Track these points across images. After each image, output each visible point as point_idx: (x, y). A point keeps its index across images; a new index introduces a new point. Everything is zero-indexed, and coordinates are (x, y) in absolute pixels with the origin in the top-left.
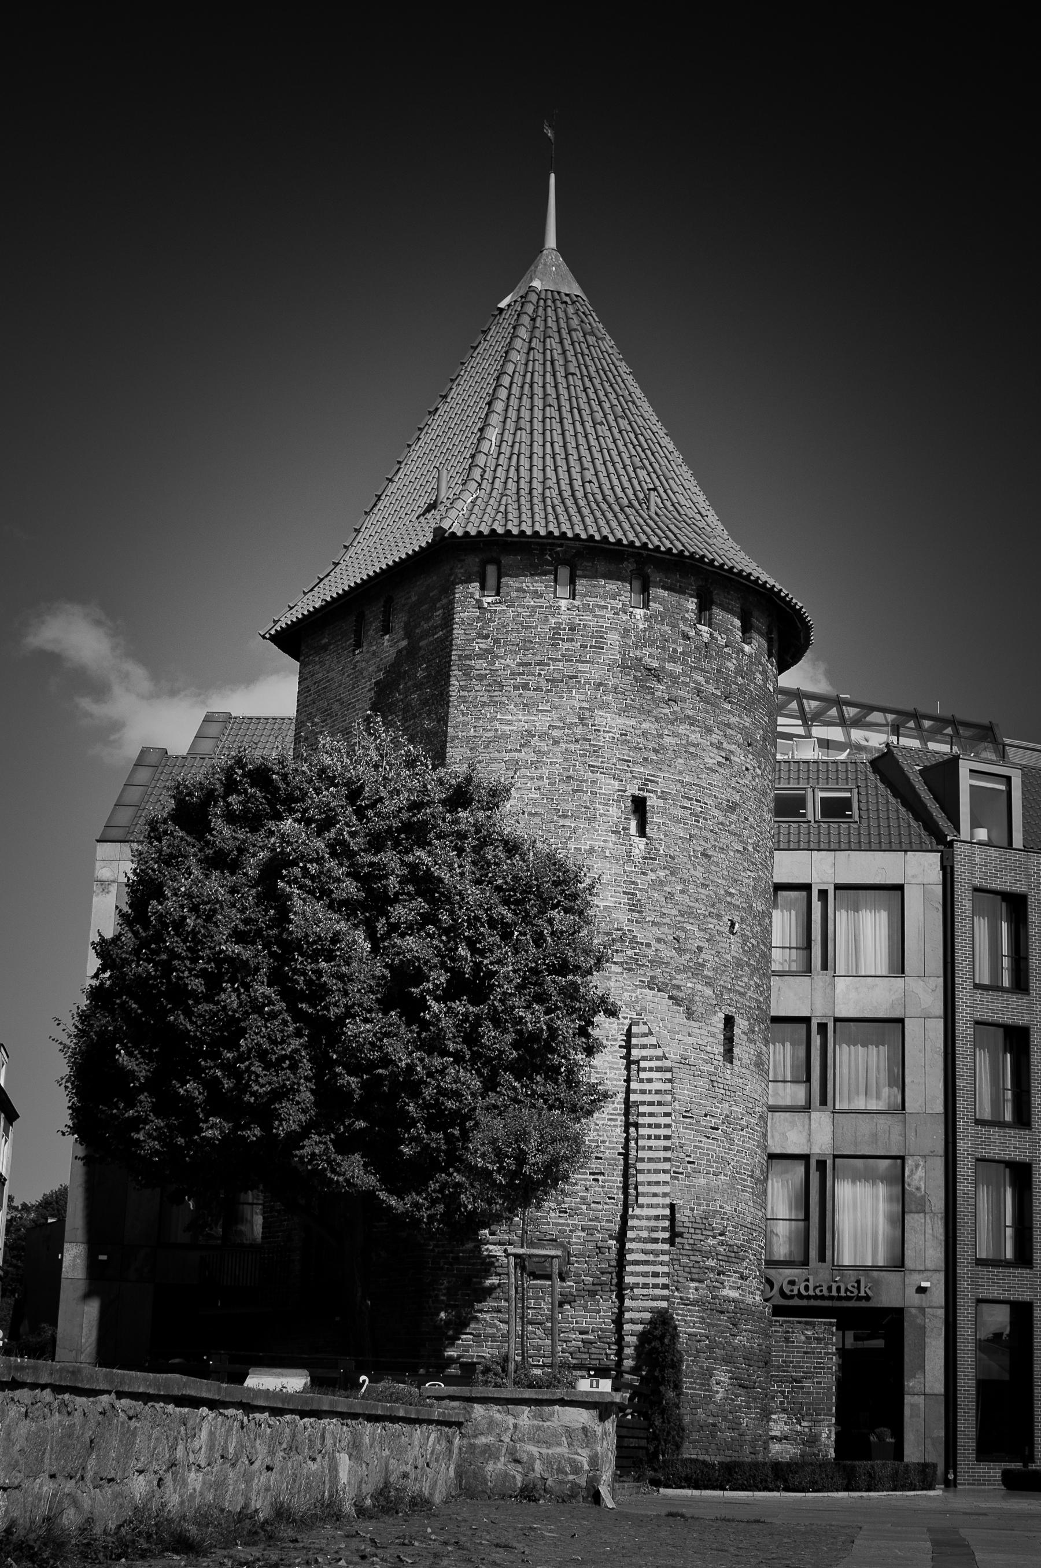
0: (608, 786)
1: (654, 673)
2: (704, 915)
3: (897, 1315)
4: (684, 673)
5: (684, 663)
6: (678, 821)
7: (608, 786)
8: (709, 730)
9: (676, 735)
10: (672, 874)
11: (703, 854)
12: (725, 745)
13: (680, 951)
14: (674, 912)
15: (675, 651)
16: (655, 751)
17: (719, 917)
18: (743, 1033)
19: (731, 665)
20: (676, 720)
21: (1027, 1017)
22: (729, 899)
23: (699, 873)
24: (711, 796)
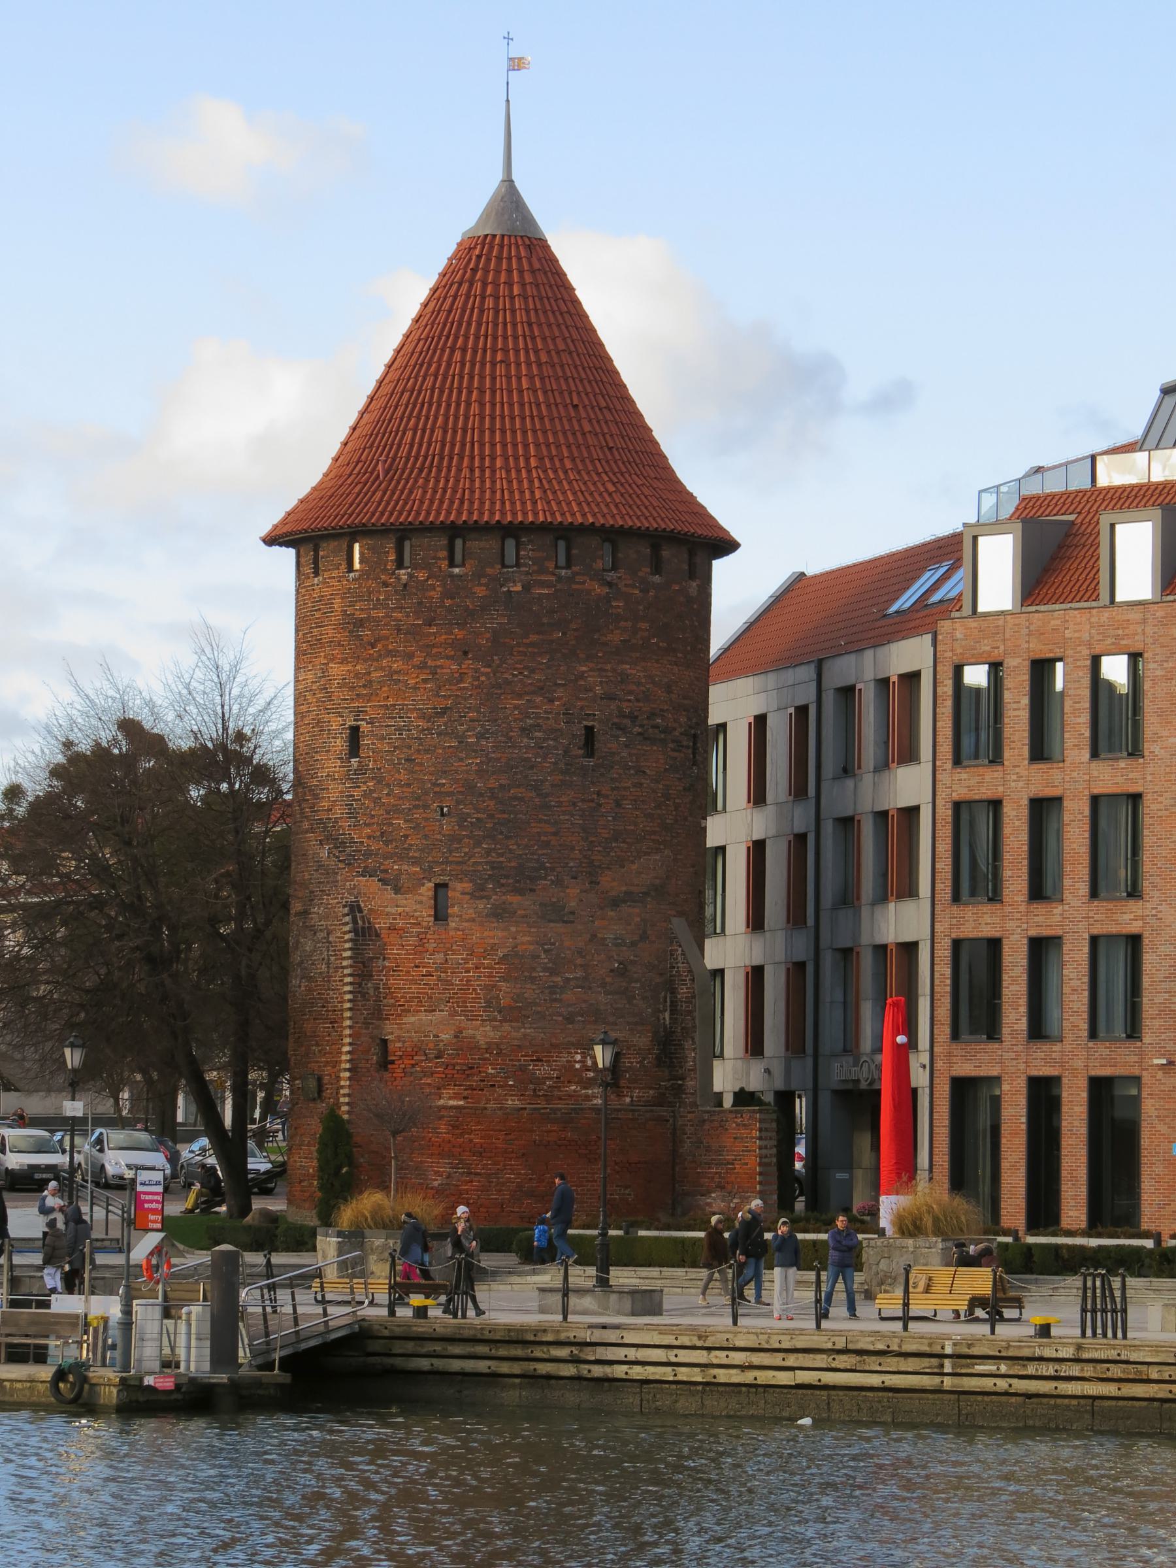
0: (336, 723)
2: (410, 810)
4: (387, 616)
5: (387, 607)
6: (383, 738)
7: (336, 723)
8: (411, 656)
9: (382, 669)
10: (379, 782)
11: (407, 760)
12: (430, 663)
13: (387, 843)
14: (381, 812)
15: (378, 600)
16: (364, 686)
17: (426, 807)
18: (463, 893)
19: (435, 595)
21: (1001, 789)
22: (437, 789)
23: (404, 776)
24: (412, 711)
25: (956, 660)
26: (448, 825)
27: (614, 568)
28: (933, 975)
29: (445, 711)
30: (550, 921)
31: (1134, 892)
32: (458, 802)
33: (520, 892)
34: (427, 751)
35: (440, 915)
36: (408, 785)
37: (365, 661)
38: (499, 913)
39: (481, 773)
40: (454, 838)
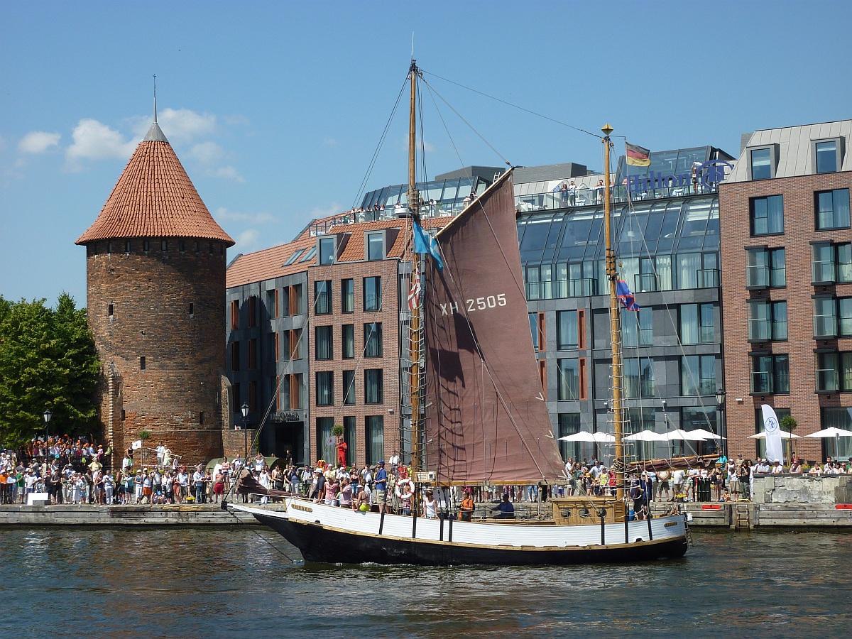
0: (104, 304)
1: (113, 270)
3: (303, 422)
12: (137, 283)
13: (124, 344)
20: (120, 281)
25: (316, 280)
26: (144, 338)
27: (198, 251)
28: (310, 382)
29: (142, 299)
30: (180, 369)
31: (379, 355)
32: (148, 330)
33: (169, 359)
34: (137, 313)
35: (143, 367)
36: (130, 324)
37: (115, 282)
38: (162, 367)
39: (156, 320)
40: (147, 342)
